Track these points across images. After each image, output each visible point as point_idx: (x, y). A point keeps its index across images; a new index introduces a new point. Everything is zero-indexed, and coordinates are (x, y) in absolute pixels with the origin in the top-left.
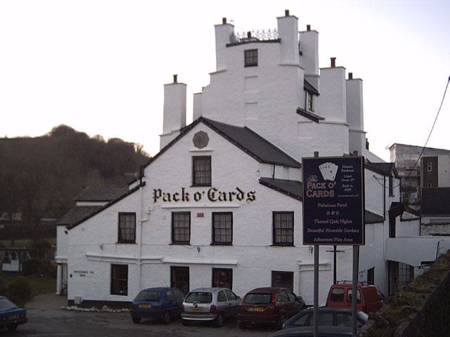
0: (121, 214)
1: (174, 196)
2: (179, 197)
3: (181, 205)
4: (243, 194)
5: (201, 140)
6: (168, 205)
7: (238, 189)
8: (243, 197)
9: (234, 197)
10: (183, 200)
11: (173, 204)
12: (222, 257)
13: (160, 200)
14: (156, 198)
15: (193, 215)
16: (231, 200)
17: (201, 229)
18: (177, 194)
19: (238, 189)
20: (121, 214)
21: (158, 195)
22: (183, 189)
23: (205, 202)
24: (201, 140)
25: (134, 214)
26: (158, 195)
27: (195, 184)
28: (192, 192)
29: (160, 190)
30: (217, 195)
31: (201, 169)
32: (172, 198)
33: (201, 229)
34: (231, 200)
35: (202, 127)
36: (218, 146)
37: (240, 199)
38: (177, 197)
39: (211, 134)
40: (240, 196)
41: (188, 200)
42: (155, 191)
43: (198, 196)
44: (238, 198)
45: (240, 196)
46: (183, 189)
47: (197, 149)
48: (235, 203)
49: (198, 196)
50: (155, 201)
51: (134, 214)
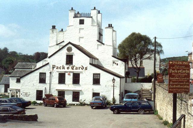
0: (40, 73)
1: (60, 67)
2: (61, 68)
3: (62, 71)
4: (83, 67)
5: (69, 50)
6: (58, 70)
7: (82, 66)
8: (83, 69)
9: (80, 69)
10: (63, 69)
11: (59, 70)
12: (76, 88)
13: (55, 69)
14: (53, 68)
15: (66, 74)
16: (79, 69)
17: (69, 79)
18: (61, 67)
19: (82, 66)
20: (40, 73)
21: (54, 67)
22: (63, 66)
23: (70, 70)
24: (69, 50)
25: (45, 73)
26: (54, 67)
27: (67, 64)
28: (66, 66)
29: (55, 66)
30: (75, 68)
31: (70, 59)
32: (59, 68)
33: (69, 79)
34: (79, 69)
35: (70, 45)
36: (74, 50)
37: (82, 69)
38: (61, 68)
39: (73, 47)
40: (82, 68)
41: (64, 69)
42: (53, 65)
43: (68, 68)
44: (82, 69)
45: (82, 68)
46: (63, 66)
47: (68, 52)
48: (81, 70)
49: (68, 68)
50: (53, 69)
51: (45, 73)
